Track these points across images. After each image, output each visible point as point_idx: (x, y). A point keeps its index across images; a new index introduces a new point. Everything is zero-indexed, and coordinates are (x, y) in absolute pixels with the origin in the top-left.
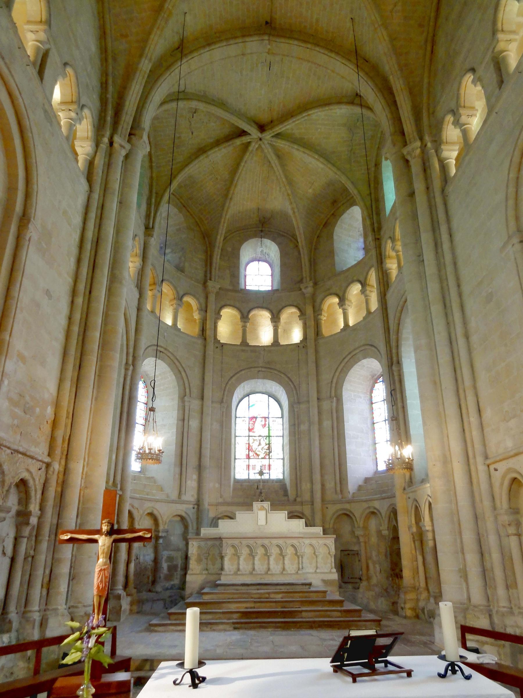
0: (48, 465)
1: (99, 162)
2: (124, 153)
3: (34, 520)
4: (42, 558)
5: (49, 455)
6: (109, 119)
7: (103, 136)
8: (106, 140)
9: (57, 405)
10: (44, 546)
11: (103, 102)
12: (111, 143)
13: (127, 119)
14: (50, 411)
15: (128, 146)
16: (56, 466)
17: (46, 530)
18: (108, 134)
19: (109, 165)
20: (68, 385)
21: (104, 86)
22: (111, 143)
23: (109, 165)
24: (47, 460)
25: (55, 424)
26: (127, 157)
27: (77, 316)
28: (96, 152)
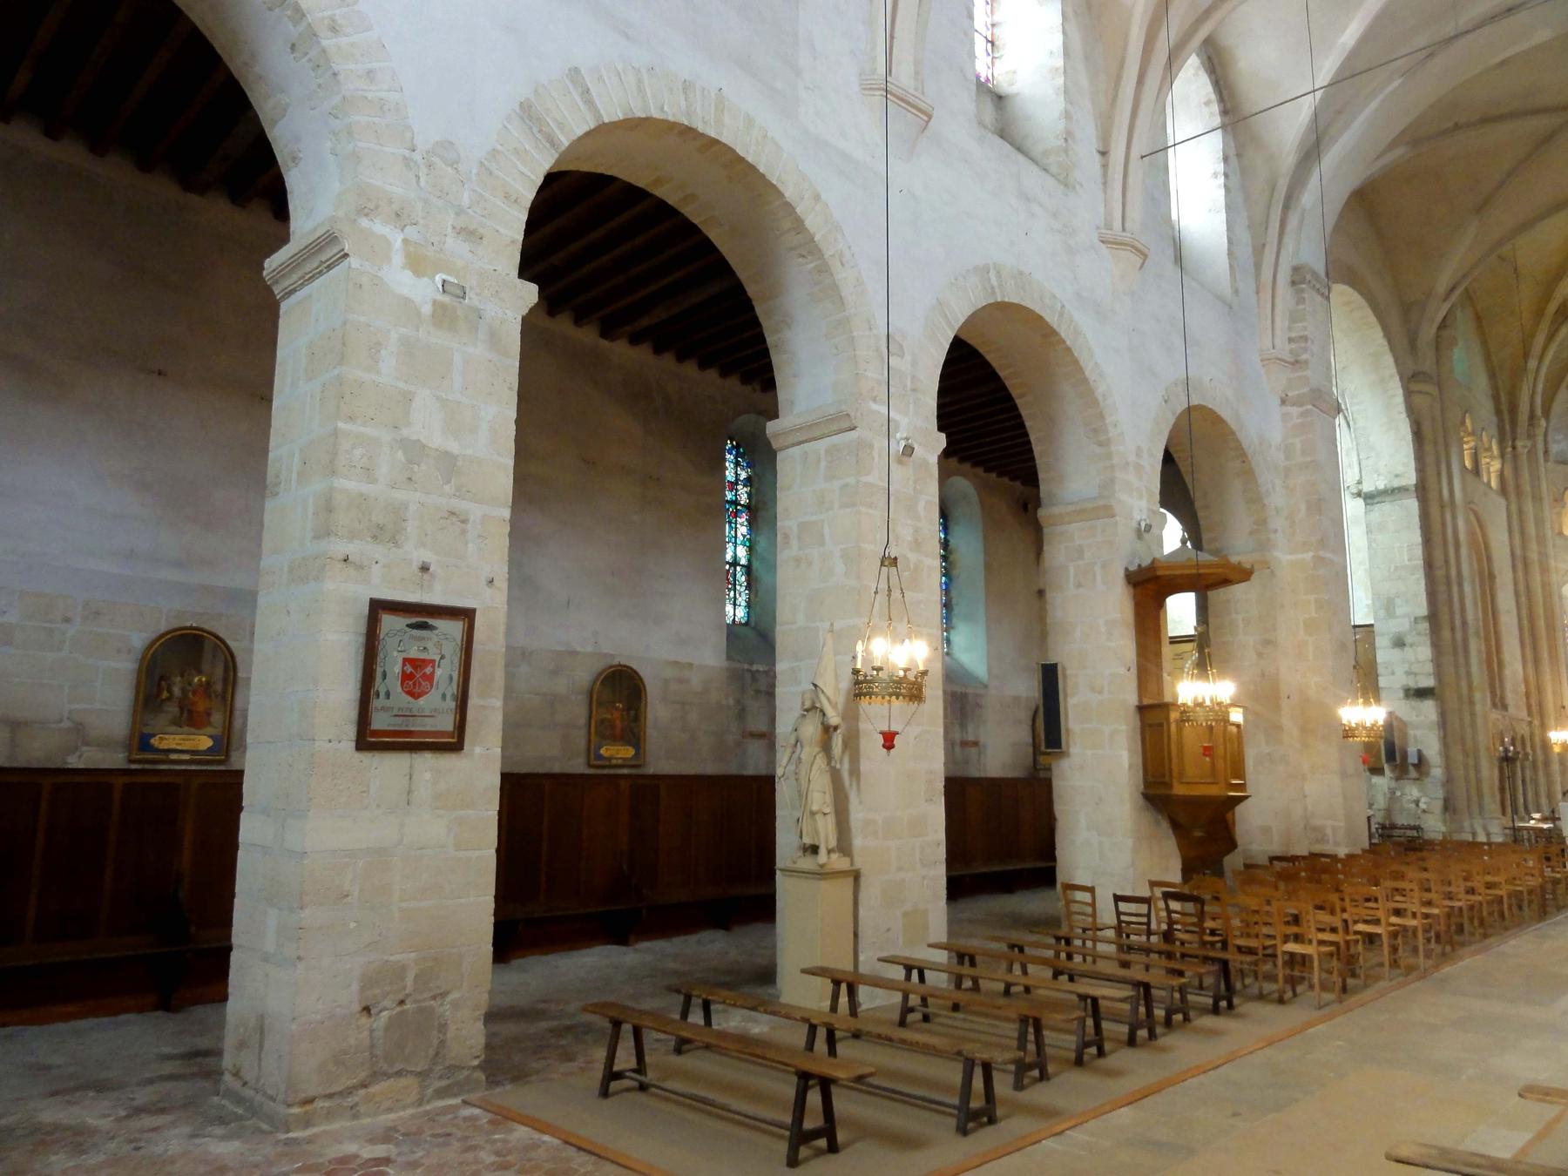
0: (1530, 723)
1: (1508, 472)
2: (1526, 450)
3: (1530, 757)
4: (1542, 780)
5: (1529, 715)
6: (1508, 427)
7: (1506, 447)
8: (1509, 449)
9: (1526, 681)
10: (1541, 773)
11: (1498, 412)
12: (1514, 448)
13: (1523, 416)
14: (1522, 688)
15: (1529, 444)
16: (1536, 722)
17: (1540, 764)
18: (1510, 443)
19: (1516, 469)
20: (1530, 665)
21: (1496, 398)
22: (1514, 448)
23: (1516, 469)
24: (1529, 719)
25: (1528, 695)
26: (1529, 452)
27: (1524, 612)
28: (1503, 465)
